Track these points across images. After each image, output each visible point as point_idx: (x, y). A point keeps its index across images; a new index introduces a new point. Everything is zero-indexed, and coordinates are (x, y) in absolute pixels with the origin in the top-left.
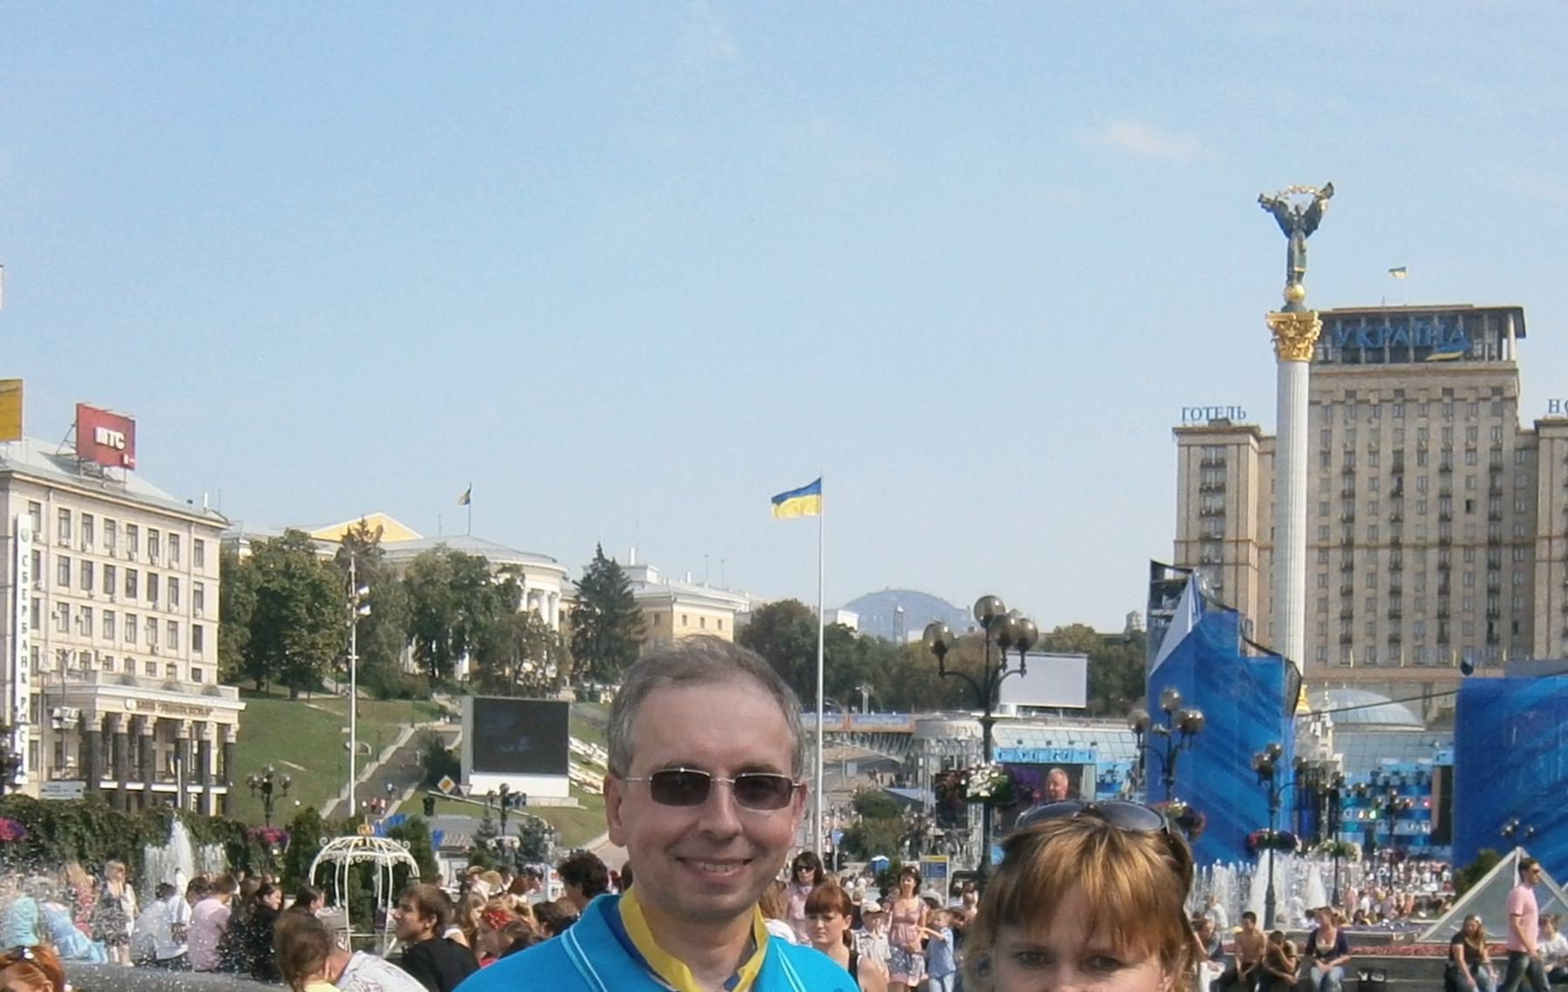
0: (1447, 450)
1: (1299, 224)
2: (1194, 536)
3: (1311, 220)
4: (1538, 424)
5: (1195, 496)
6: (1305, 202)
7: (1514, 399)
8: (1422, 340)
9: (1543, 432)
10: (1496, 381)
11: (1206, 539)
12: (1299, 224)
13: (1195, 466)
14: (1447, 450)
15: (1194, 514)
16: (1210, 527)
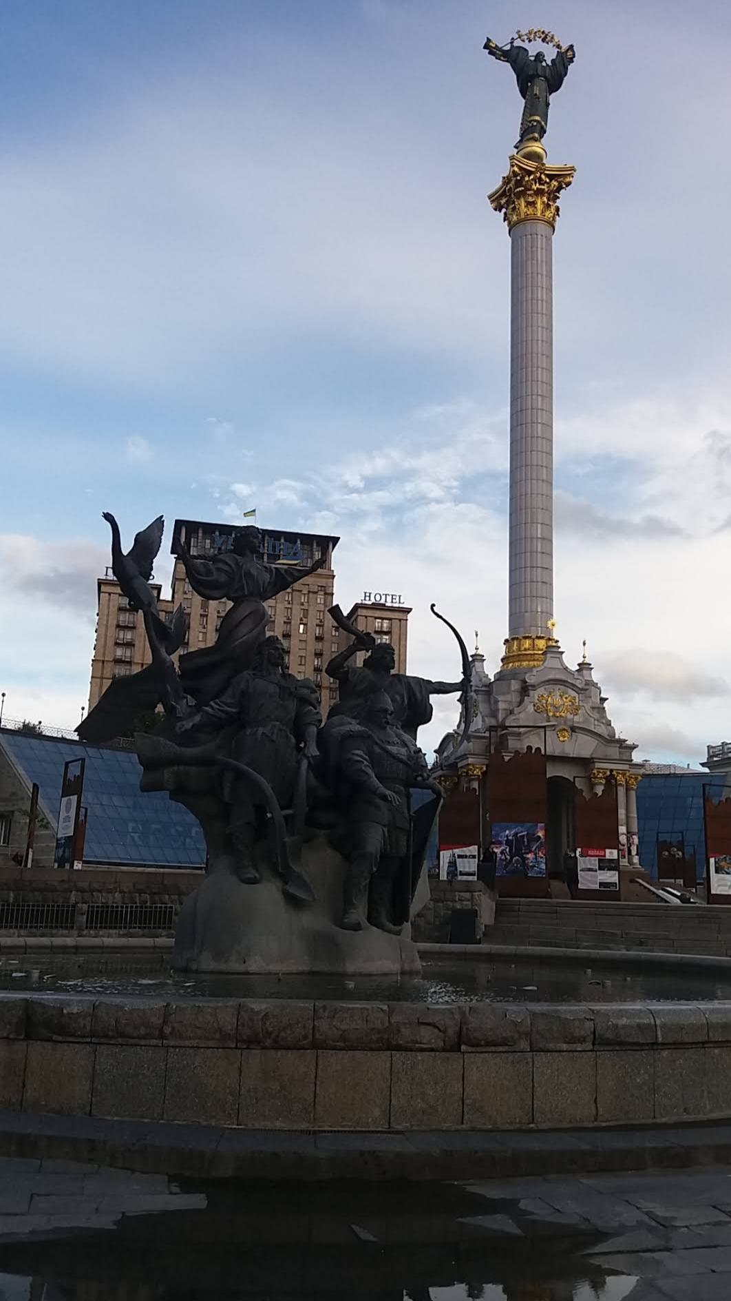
0: (288, 623)
1: (539, 77)
2: (109, 658)
3: (555, 76)
4: (357, 607)
5: (112, 631)
6: (550, 54)
7: (332, 594)
8: (274, 547)
9: (360, 612)
10: (322, 582)
11: (118, 661)
12: (539, 77)
13: (114, 609)
14: (288, 623)
15: (110, 643)
16: (119, 652)
